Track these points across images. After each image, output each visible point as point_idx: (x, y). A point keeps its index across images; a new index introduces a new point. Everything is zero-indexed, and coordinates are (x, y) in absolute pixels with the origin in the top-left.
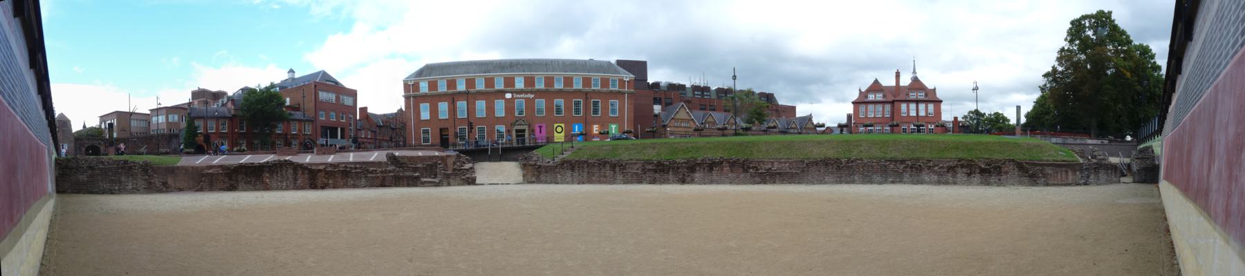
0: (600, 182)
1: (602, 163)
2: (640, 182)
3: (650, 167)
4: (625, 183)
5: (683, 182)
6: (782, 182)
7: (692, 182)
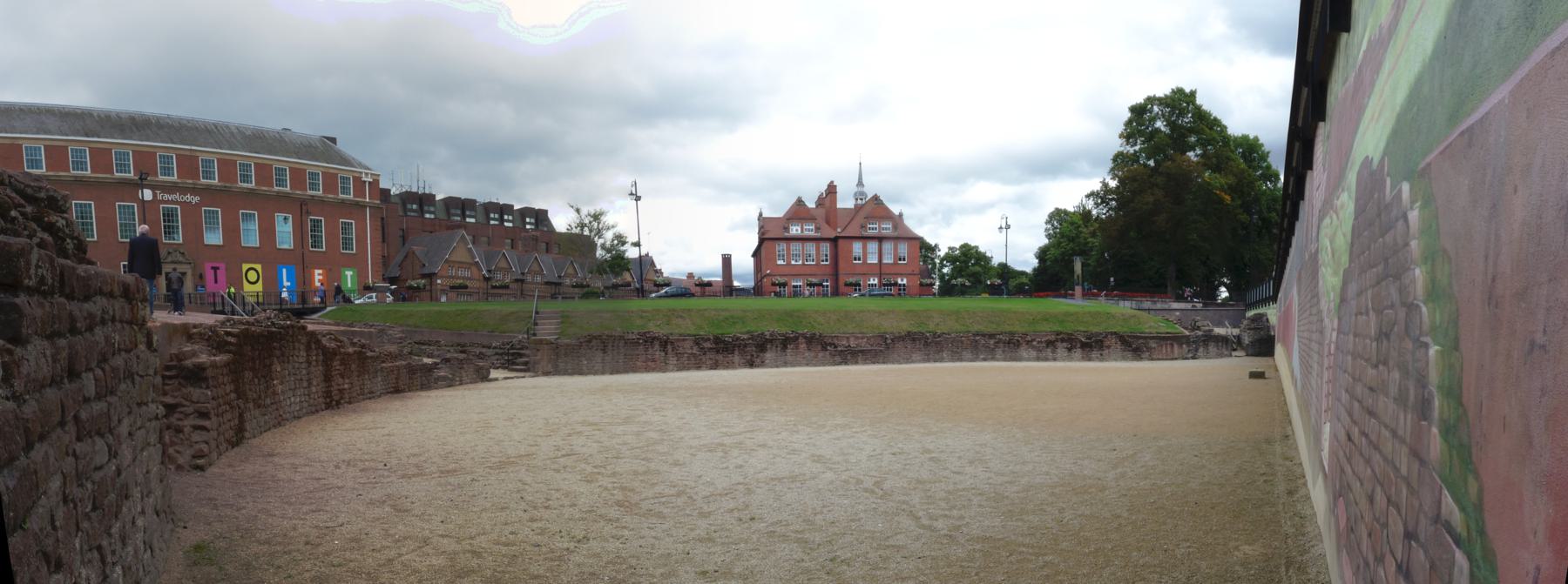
0: (647, 369)
1: (649, 340)
2: (699, 368)
3: (707, 345)
4: (681, 368)
5: (751, 365)
6: (865, 362)
7: (762, 364)
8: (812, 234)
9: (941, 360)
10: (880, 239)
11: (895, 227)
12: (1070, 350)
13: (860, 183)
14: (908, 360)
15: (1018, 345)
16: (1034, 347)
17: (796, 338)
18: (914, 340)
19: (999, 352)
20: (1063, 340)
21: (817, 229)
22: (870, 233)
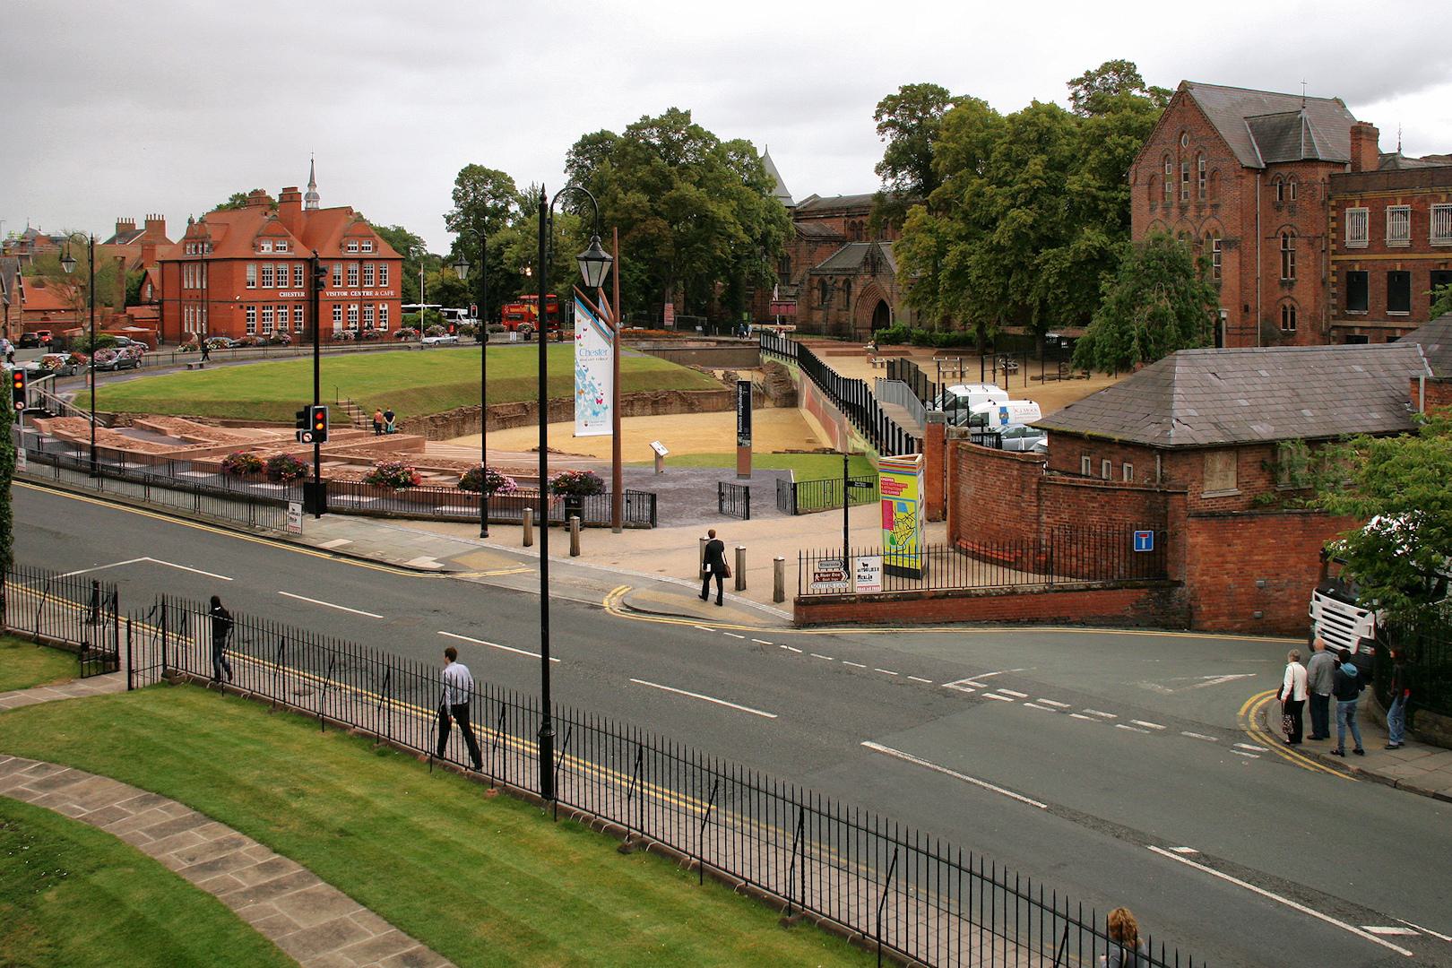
5: (459, 435)
10: (361, 261)
12: (643, 407)
21: (291, 247)
22: (352, 253)
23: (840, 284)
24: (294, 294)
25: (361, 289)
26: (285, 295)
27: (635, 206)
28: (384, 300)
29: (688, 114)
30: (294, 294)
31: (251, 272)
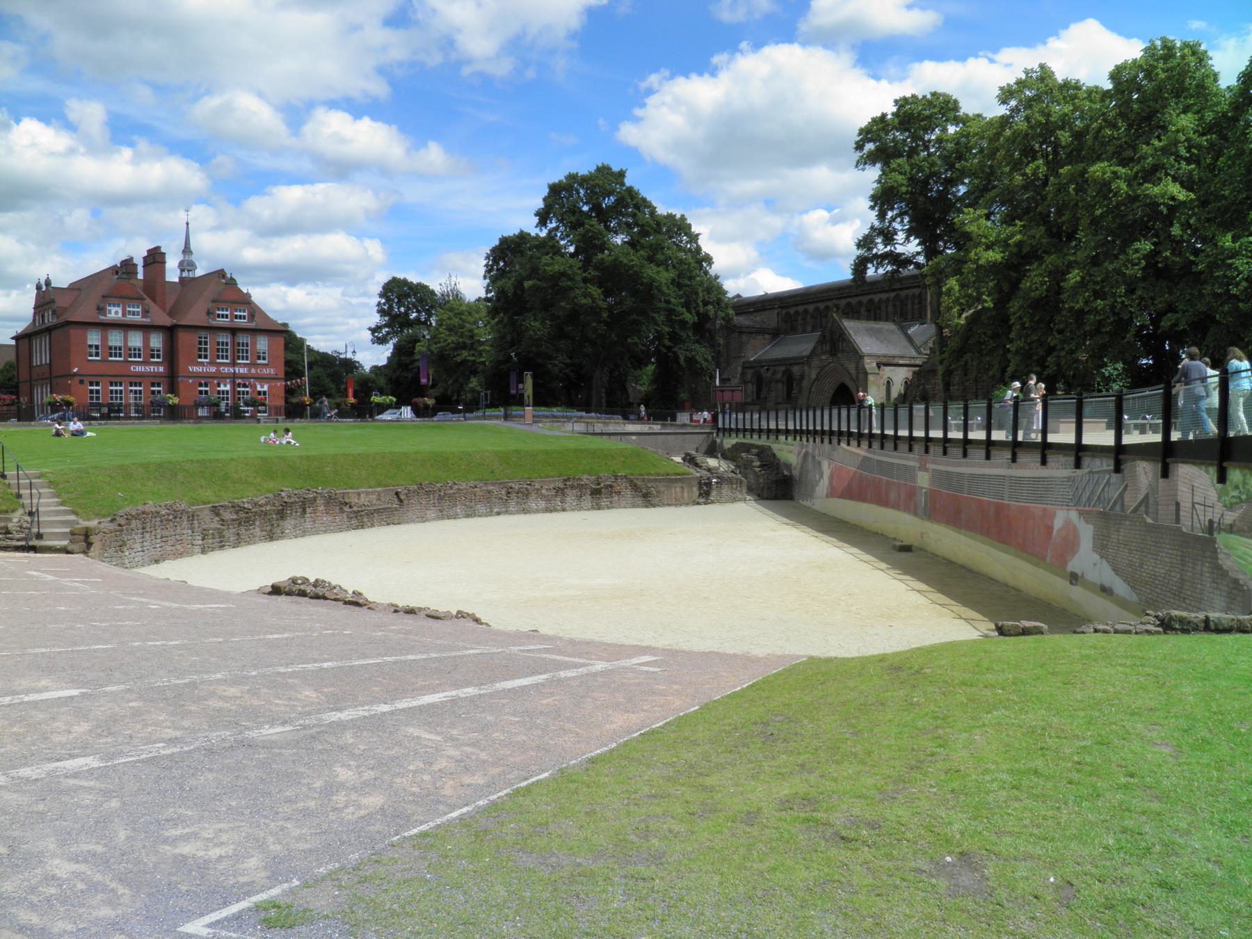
5: (271, 537)
7: (282, 536)
8: (138, 319)
9: (455, 517)
10: (234, 331)
11: (252, 317)
13: (187, 250)
14: (423, 519)
15: (527, 495)
16: (543, 497)
17: (315, 499)
18: (428, 493)
19: (512, 505)
20: (572, 487)
21: (145, 313)
23: (779, 376)
24: (152, 369)
25: (234, 364)
26: (139, 369)
27: (563, 274)
28: (262, 379)
29: (622, 174)
30: (152, 369)
31: (94, 338)
